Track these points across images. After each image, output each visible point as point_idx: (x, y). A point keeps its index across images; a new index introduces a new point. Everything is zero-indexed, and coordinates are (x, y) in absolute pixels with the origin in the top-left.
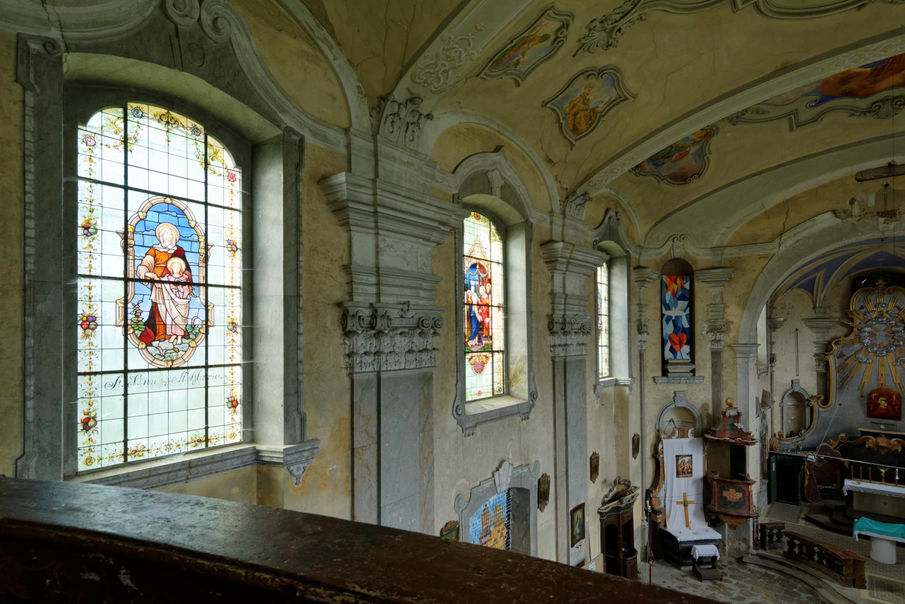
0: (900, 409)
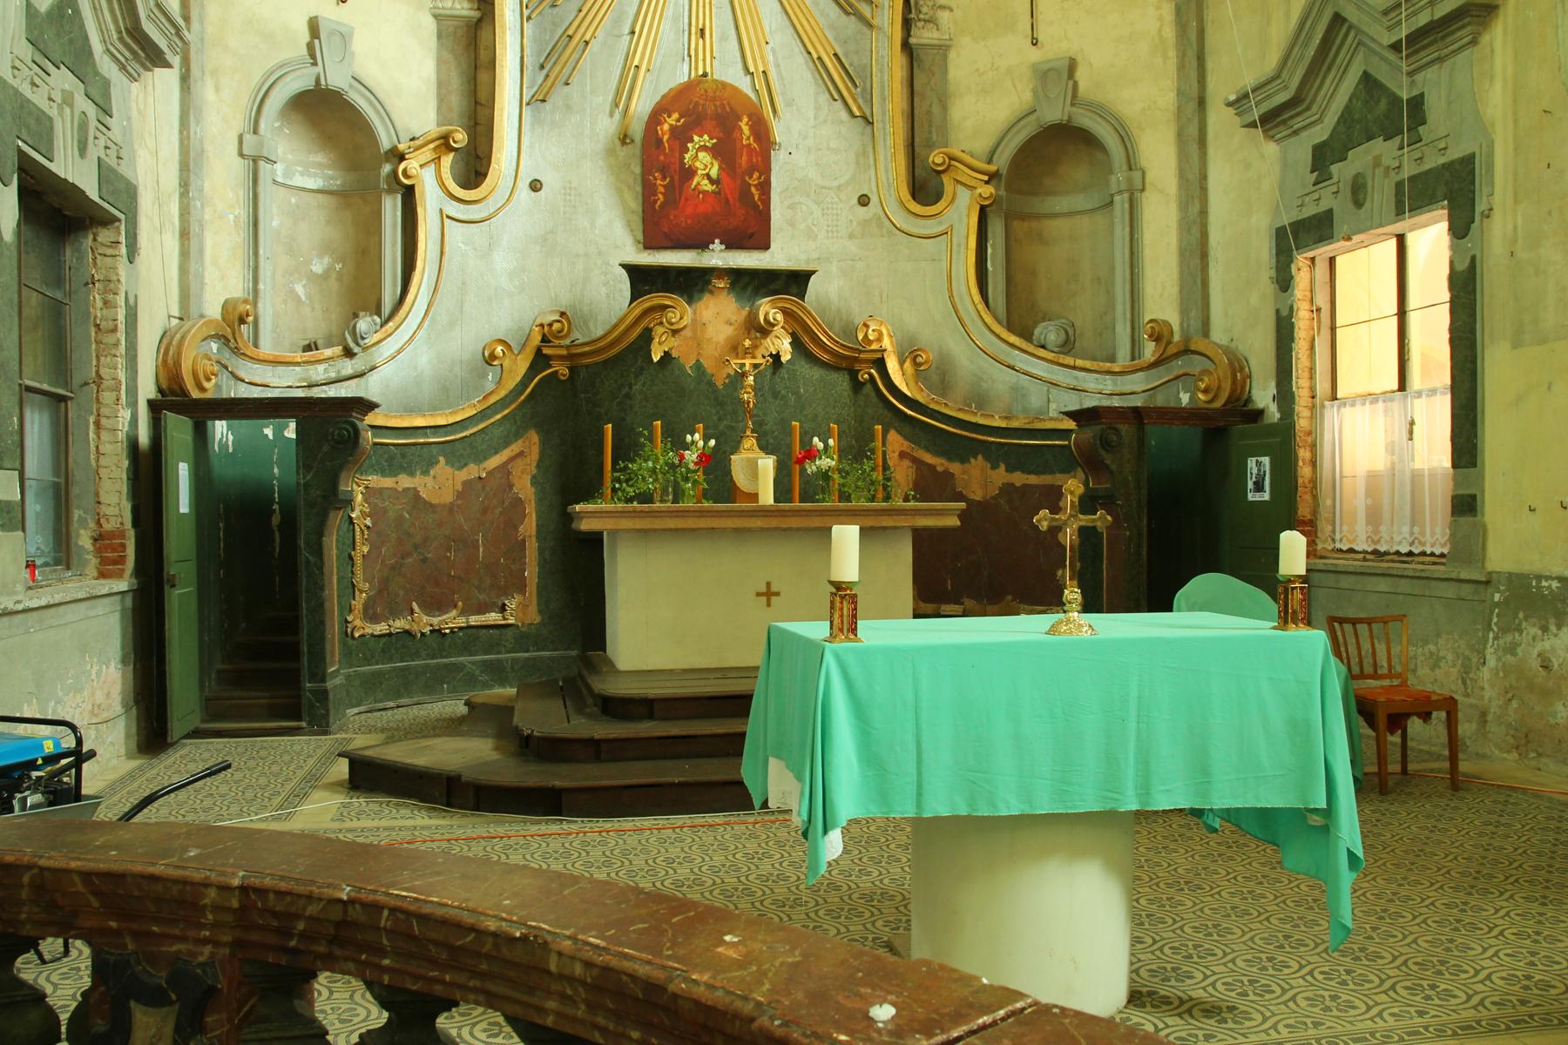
0: (765, 187)
